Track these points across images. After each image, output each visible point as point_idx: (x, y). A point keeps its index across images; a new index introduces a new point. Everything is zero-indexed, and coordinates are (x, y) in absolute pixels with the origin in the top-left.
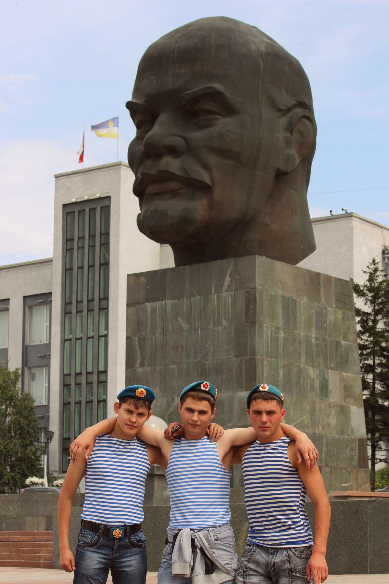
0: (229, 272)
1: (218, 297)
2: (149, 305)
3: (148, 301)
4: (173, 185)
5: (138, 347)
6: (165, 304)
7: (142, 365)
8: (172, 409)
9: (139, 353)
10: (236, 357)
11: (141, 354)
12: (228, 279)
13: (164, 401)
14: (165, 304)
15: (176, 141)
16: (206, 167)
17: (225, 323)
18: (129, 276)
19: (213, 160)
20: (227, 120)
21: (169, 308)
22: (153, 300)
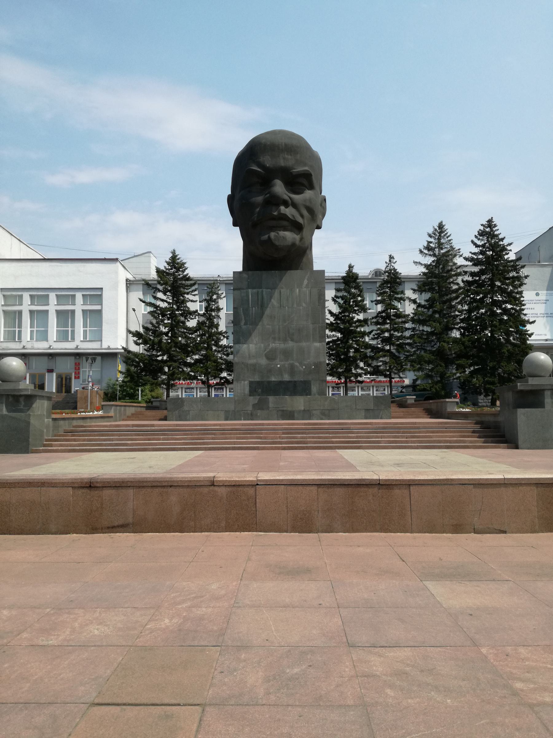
0: (306, 277)
1: (299, 290)
2: (250, 290)
3: (248, 287)
4: (285, 223)
5: (242, 313)
6: (262, 291)
7: (246, 324)
8: (268, 350)
9: (243, 318)
10: (313, 324)
11: (245, 318)
12: (306, 282)
13: (262, 345)
14: (262, 291)
15: (286, 197)
16: (302, 216)
17: (304, 305)
18: (234, 272)
19: (305, 213)
20: (309, 191)
21: (264, 293)
22: (253, 288)
